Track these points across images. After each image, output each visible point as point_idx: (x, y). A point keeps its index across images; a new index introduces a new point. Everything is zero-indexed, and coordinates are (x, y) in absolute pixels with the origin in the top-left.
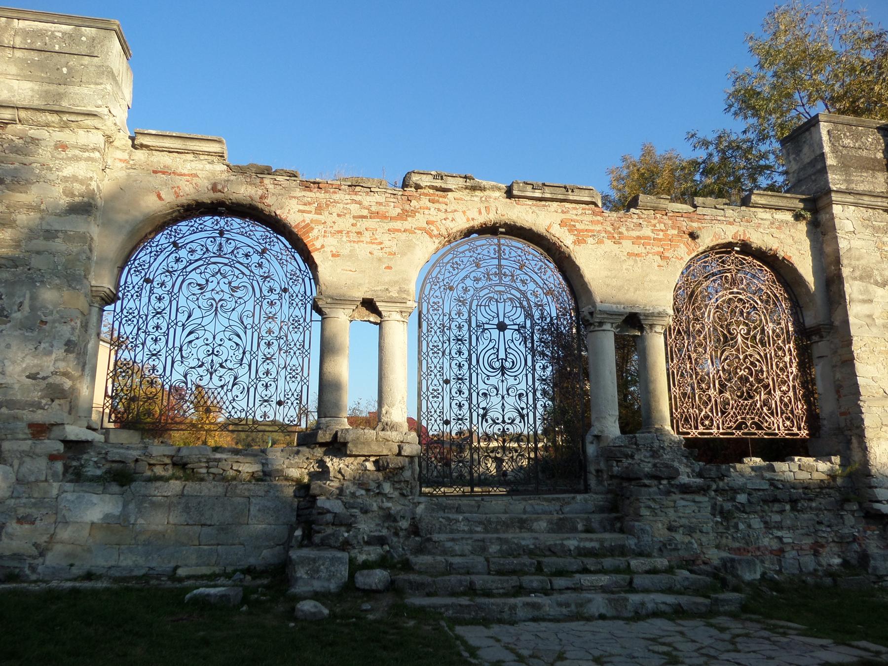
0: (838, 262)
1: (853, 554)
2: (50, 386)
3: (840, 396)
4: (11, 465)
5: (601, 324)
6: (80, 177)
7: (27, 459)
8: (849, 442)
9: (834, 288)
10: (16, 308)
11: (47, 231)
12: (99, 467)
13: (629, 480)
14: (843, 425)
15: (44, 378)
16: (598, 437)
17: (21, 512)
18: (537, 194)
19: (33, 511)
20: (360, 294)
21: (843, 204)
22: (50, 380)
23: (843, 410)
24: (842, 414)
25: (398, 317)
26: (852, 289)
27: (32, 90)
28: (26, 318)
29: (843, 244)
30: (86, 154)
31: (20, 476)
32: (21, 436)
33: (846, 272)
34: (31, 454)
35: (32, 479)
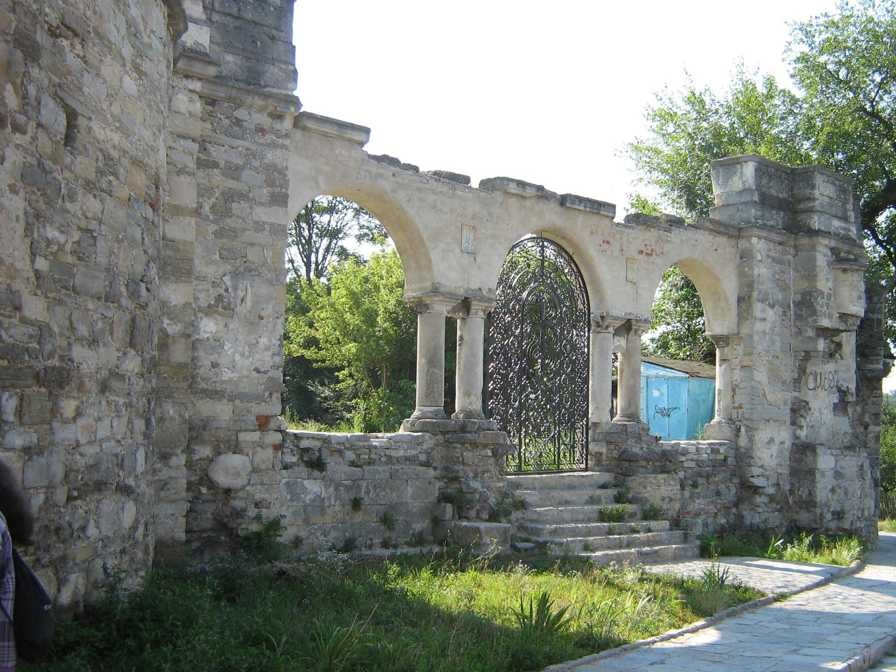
0: (751, 286)
1: (732, 516)
2: (271, 379)
3: (735, 394)
4: (247, 455)
5: (607, 327)
6: (279, 166)
7: (258, 449)
8: (739, 430)
9: (744, 307)
10: (239, 302)
11: (256, 222)
12: (294, 455)
13: (629, 461)
14: (734, 416)
15: (265, 372)
16: (595, 424)
17: (258, 497)
18: (581, 208)
19: (266, 496)
20: (461, 292)
21: (760, 238)
22: (270, 374)
23: (736, 405)
24: (734, 408)
25: (481, 314)
26: (758, 308)
27: (236, 64)
28: (249, 312)
29: (756, 272)
30: (281, 141)
31: (255, 465)
32: (252, 428)
33: (755, 294)
34: (262, 446)
35: (263, 467)
